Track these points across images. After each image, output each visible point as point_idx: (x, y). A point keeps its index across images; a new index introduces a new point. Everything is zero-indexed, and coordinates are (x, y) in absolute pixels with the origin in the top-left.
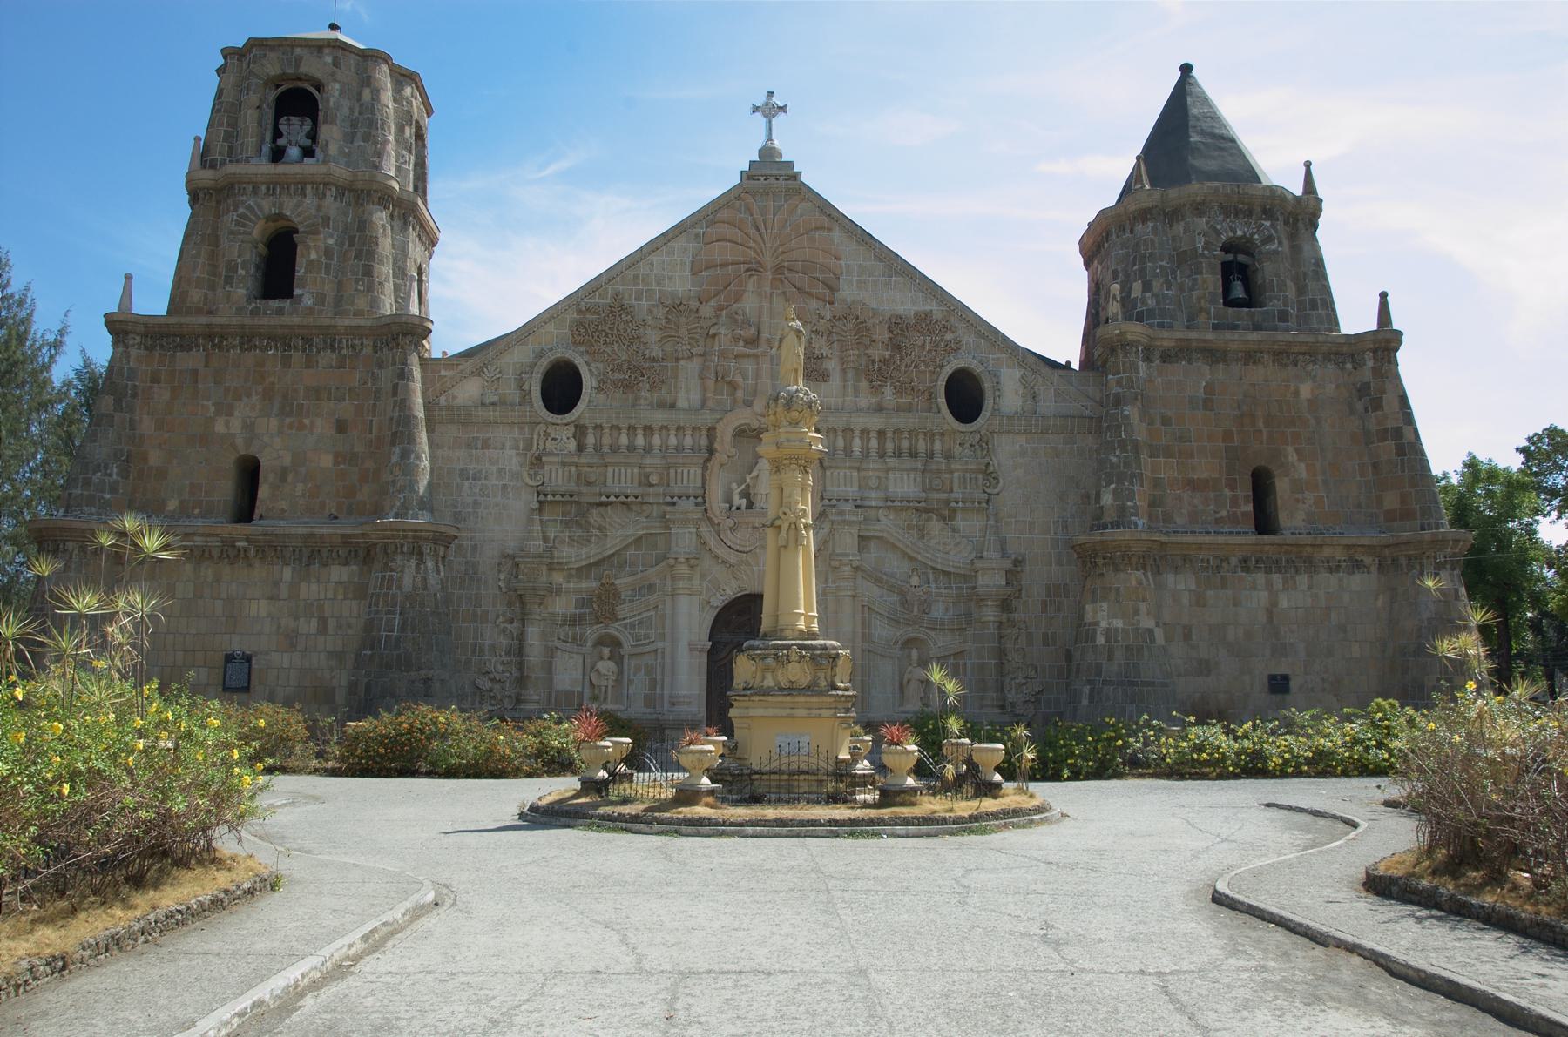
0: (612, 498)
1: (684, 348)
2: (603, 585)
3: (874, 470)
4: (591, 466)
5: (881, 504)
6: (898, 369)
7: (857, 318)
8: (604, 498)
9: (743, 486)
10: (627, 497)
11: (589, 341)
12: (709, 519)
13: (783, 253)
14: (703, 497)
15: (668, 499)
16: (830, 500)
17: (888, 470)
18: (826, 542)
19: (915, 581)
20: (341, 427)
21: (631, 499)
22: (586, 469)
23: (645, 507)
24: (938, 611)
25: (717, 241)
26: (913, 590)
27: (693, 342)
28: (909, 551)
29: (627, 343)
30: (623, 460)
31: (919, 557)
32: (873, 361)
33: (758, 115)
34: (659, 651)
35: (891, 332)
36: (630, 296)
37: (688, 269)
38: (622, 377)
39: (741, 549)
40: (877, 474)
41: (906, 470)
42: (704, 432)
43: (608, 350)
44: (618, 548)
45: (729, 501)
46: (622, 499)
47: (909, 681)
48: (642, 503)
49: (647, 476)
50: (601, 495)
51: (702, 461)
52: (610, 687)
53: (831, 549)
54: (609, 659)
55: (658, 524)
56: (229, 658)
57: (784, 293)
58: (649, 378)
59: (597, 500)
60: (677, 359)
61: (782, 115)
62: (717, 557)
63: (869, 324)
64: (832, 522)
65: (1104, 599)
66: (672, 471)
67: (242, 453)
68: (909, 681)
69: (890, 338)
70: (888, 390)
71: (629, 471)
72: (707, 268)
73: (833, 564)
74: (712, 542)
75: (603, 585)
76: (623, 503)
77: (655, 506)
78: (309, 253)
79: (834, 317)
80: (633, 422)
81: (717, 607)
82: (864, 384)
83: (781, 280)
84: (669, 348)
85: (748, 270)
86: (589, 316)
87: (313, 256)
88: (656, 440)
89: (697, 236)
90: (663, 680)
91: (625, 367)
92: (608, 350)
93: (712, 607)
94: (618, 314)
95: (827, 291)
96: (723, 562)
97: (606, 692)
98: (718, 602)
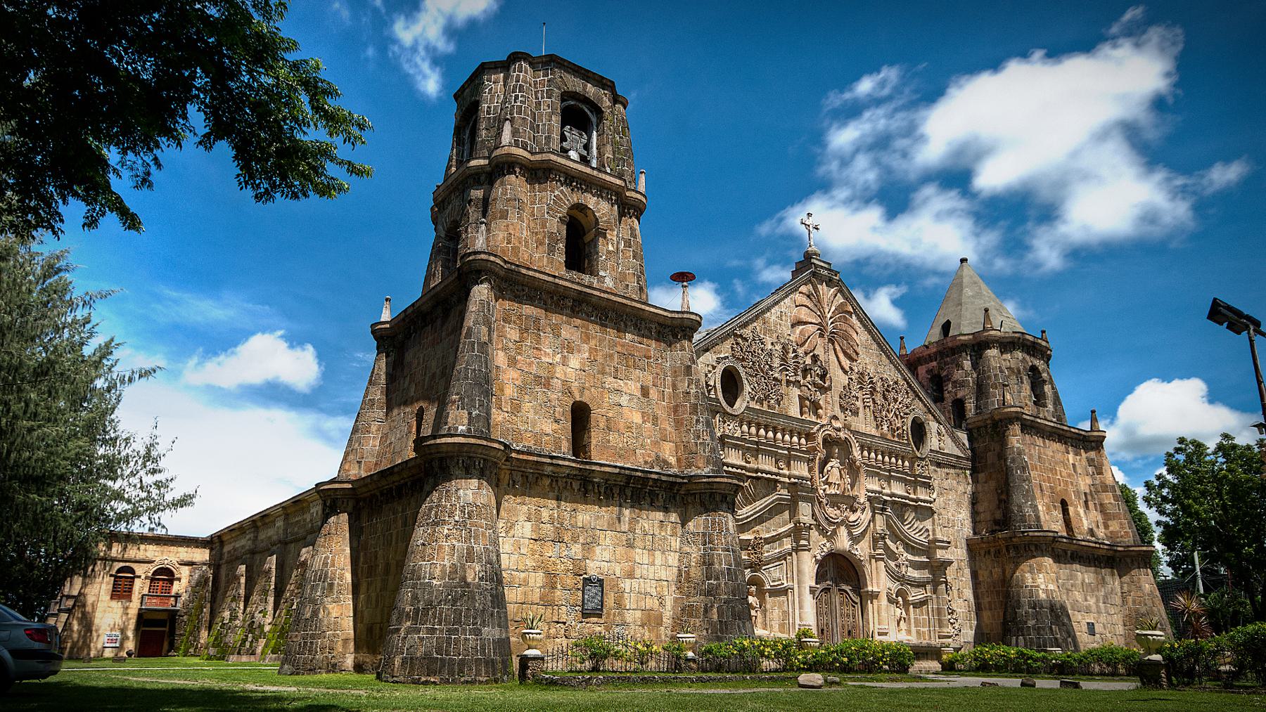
2: (756, 538)
6: (888, 411)
8: (759, 474)
13: (832, 323)
15: (792, 480)
20: (645, 392)
21: (774, 477)
24: (914, 574)
48: (776, 481)
56: (588, 581)
63: (875, 381)
65: (1039, 571)
67: (578, 399)
78: (607, 244)
87: (611, 248)
96: (823, 530)
98: (819, 557)
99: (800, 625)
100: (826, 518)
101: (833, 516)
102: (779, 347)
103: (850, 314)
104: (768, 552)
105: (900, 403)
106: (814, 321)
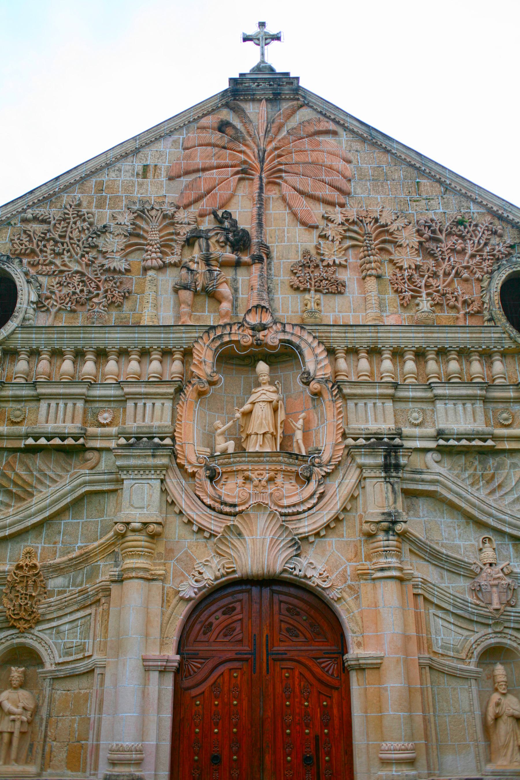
0: (43, 441)
1: (154, 255)
2: (19, 567)
3: (415, 400)
4: (17, 399)
5: (432, 445)
6: (435, 275)
7: (376, 220)
8: (30, 441)
9: (231, 423)
10: (63, 439)
11: (33, 251)
12: (181, 467)
14: (173, 438)
15: (123, 441)
16: (355, 439)
17: (437, 398)
18: (353, 498)
19: (489, 554)
21: (70, 441)
22: (11, 405)
23: (89, 455)
25: (199, 146)
26: (488, 570)
27: (166, 250)
28: (476, 513)
29: (80, 253)
30: (62, 391)
31: (491, 522)
32: (401, 268)
33: (250, 44)
34: (97, 671)
35: (421, 235)
36: (90, 203)
37: (164, 173)
38: (71, 290)
39: (227, 509)
40: (419, 405)
41: (460, 398)
42: (177, 356)
43: (58, 262)
44: (47, 514)
45: (211, 444)
46: (57, 441)
47: (497, 718)
48: (83, 449)
49: (95, 415)
50: (27, 436)
51: (172, 390)
52: (16, 734)
53: (360, 511)
54: (22, 686)
55: (106, 477)
57: (284, 199)
58: (106, 291)
59: (22, 444)
60: (146, 269)
61: (275, 42)
62: (190, 523)
63: (393, 228)
64: (361, 467)
66: (130, 405)
68: (497, 718)
69: (420, 243)
70: (425, 305)
71: (70, 405)
72: (187, 173)
73: (366, 527)
74: (183, 502)
75: (19, 567)
76: (59, 449)
77: (104, 454)
79: (347, 220)
80: (80, 344)
81: (190, 599)
82: (390, 295)
83: (279, 184)
84: (136, 258)
85: (237, 173)
86: (37, 228)
88: (111, 365)
89: (175, 141)
90: (100, 720)
91: (77, 278)
92: (58, 262)
93: (182, 599)
94: (72, 220)
95: (336, 194)
97: (10, 742)
99: (112, 751)
100: (209, 507)
101: (236, 501)
102: (126, 219)
103: (335, 133)
104: (60, 593)
105: (473, 256)
106: (228, 161)
